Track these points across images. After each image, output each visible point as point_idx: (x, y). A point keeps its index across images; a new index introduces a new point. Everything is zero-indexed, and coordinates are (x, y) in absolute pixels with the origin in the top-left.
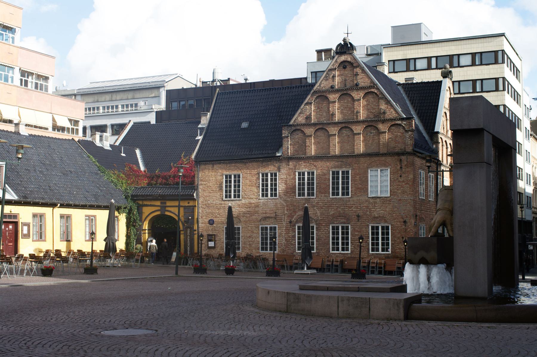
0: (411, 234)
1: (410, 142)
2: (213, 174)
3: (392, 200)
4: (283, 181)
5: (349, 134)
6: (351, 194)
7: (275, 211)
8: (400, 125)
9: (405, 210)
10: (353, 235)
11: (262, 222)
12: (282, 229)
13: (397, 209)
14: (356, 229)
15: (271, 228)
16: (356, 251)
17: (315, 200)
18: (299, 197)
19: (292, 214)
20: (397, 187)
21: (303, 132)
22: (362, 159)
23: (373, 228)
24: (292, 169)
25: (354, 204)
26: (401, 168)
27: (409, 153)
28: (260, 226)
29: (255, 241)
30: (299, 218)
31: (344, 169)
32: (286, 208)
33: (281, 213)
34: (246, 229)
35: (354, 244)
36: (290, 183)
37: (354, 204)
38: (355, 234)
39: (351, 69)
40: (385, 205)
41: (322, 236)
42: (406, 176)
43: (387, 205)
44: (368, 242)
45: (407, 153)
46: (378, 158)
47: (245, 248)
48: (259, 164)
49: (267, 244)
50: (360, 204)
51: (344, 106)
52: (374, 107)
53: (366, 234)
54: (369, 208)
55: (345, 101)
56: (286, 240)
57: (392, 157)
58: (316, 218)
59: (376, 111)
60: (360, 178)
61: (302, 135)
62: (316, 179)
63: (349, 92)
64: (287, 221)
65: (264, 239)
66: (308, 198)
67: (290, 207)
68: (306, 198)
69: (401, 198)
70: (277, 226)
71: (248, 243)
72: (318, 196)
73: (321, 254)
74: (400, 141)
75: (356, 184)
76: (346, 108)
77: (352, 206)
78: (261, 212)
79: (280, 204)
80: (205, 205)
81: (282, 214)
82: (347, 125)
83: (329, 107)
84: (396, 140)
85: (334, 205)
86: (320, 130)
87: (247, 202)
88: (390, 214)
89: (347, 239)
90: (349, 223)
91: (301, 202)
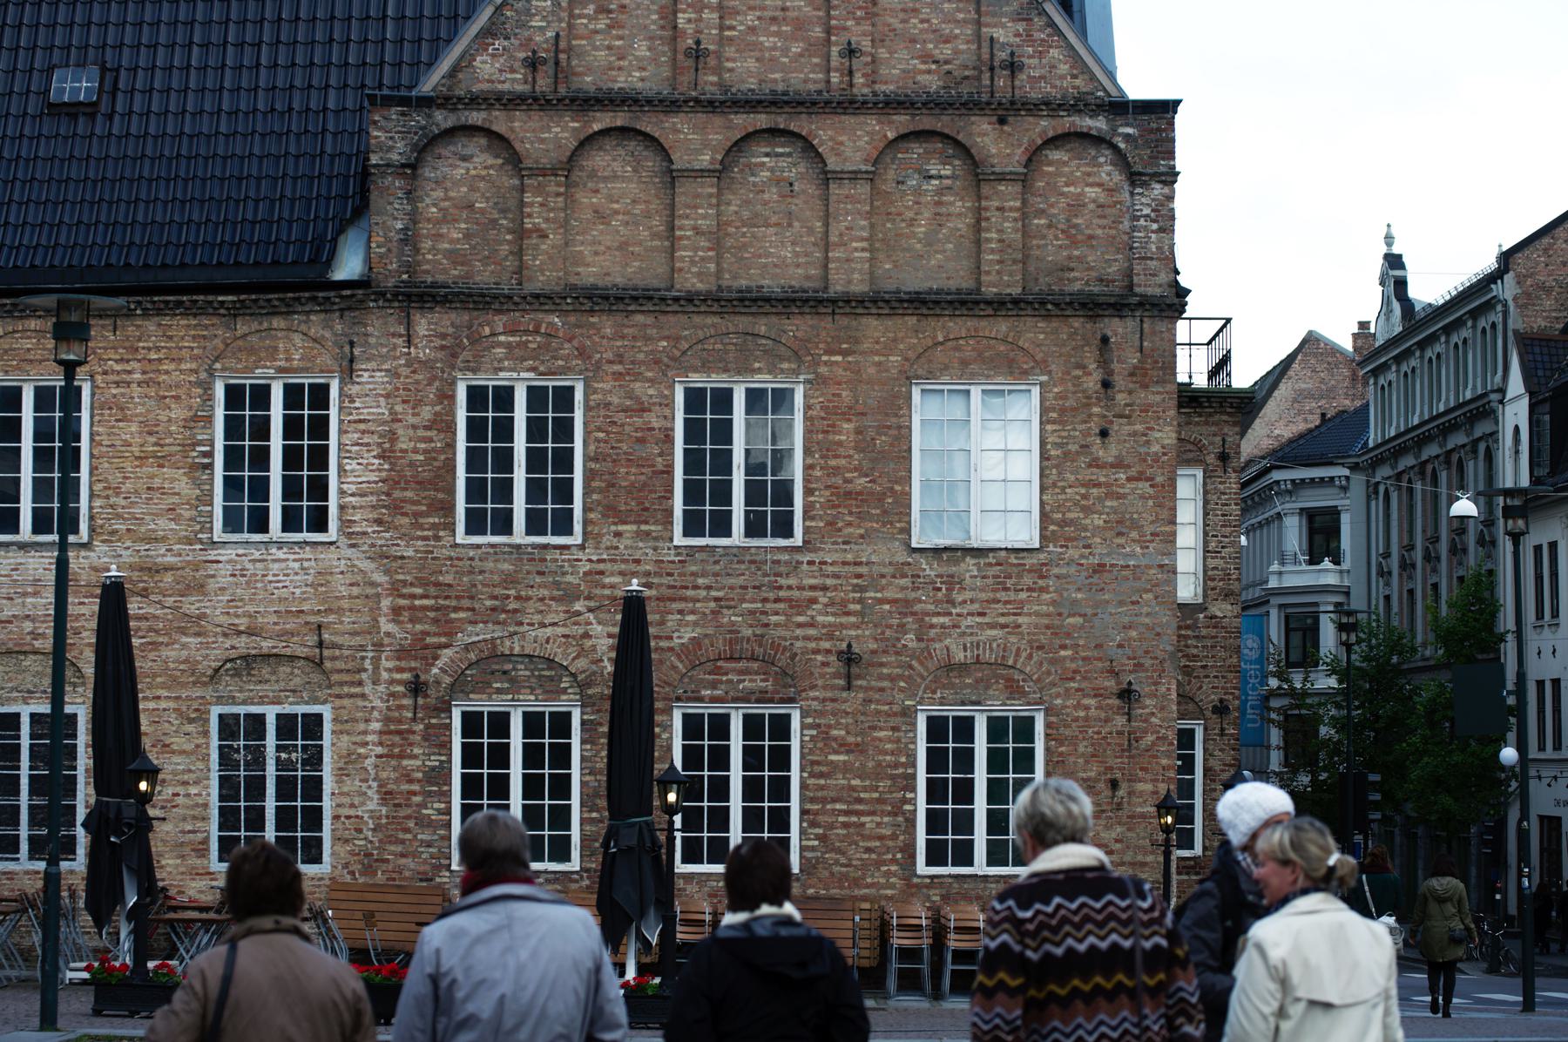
0: (1164, 762)
1: (1160, 240)
3: (1056, 571)
5: (792, 174)
6: (806, 531)
7: (312, 619)
8: (1098, 140)
10: (817, 769)
11: (228, 685)
13: (1080, 620)
14: (835, 732)
15: (286, 725)
16: (837, 862)
17: (580, 555)
19: (429, 640)
20: (1084, 497)
21: (498, 141)
22: (873, 322)
23: (936, 728)
24: (427, 364)
25: (825, 588)
26: (1106, 385)
27: (1153, 305)
28: (215, 711)
29: (180, 800)
30: (470, 666)
32: (386, 603)
33: (354, 634)
35: (821, 818)
36: (415, 451)
37: (825, 588)
40: (1012, 596)
42: (1135, 434)
43: (1023, 595)
44: (907, 807)
45: (1141, 304)
46: (970, 323)
48: (206, 327)
50: (862, 589)
52: (947, 29)
53: (896, 765)
54: (913, 614)
56: (386, 796)
57: (1055, 324)
58: (582, 663)
59: (956, 52)
60: (858, 432)
61: (490, 161)
62: (587, 433)
64: (392, 682)
66: (534, 546)
67: (413, 596)
68: (519, 547)
69: (1107, 561)
70: (327, 712)
72: (600, 535)
74: (1099, 232)
76: (774, 19)
79: (349, 578)
81: (358, 640)
83: (675, 13)
84: (1076, 226)
85: (696, 587)
86: (609, 143)
88: (1040, 648)
89: (781, 789)
90: (791, 700)
91: (490, 565)
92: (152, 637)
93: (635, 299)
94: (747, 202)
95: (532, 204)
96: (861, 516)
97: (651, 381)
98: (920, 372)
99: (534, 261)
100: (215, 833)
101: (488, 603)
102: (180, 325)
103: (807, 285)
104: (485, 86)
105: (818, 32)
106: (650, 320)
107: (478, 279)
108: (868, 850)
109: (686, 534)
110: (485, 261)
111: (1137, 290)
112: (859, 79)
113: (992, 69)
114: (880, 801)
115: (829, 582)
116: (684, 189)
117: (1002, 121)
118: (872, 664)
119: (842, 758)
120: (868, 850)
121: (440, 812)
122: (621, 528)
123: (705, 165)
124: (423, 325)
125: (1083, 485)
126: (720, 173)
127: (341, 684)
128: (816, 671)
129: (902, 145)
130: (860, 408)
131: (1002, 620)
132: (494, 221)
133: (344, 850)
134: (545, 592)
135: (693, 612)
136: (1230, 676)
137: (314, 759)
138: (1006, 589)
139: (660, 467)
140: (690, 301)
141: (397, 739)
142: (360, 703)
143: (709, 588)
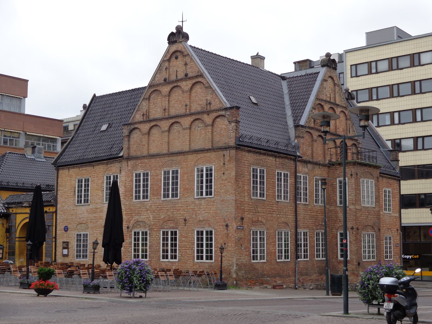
2: (69, 179)
3: (216, 201)
8: (223, 116)
13: (219, 211)
18: (136, 201)
19: (130, 219)
20: (221, 186)
23: (198, 232)
24: (130, 170)
25: (182, 207)
26: (224, 164)
31: (174, 168)
35: (181, 251)
37: (182, 207)
41: (153, 243)
42: (228, 173)
43: (211, 206)
44: (193, 248)
45: (229, 147)
46: (204, 154)
48: (104, 167)
50: (187, 207)
53: (192, 240)
57: (216, 153)
58: (149, 222)
60: (187, 177)
62: (150, 180)
63: (179, 84)
64: (125, 227)
69: (224, 199)
73: (153, 263)
75: (184, 185)
76: (177, 101)
77: (180, 209)
80: (62, 211)
85: (164, 208)
86: (155, 128)
88: (213, 217)
90: (177, 228)
91: (137, 205)
95: (143, 140)
96: (188, 193)
97: (159, 170)
98: (197, 165)
104: (137, 120)
108: (188, 257)
112: (187, 110)
113: (207, 105)
114: (189, 247)
115: (183, 205)
117: (208, 115)
118: (188, 221)
119: (184, 239)
120: (188, 257)
123: (166, 130)
124: (130, 163)
125: (220, 184)
126: (169, 131)
129: (195, 122)
130: (188, 172)
131: (208, 211)
132: (140, 144)
134: (144, 210)
135: (164, 212)
136: (354, 221)
138: (208, 205)
143: (166, 208)
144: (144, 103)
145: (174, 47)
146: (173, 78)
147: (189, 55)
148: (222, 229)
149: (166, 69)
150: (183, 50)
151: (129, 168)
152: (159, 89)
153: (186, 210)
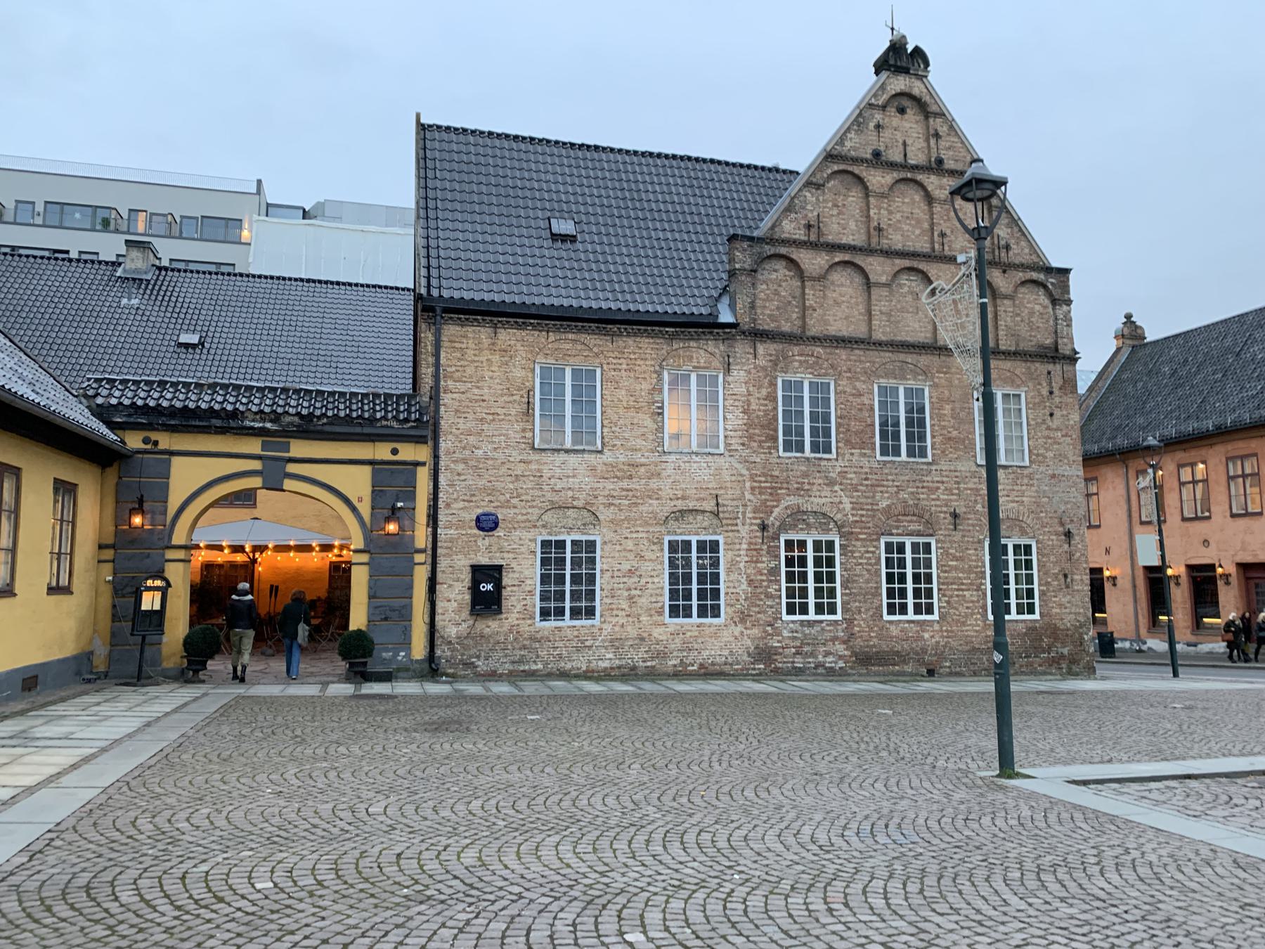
3: (1037, 477)
4: (736, 404)
6: (933, 455)
7: (714, 492)
9: (1066, 503)
10: (944, 568)
12: (738, 547)
14: (951, 551)
15: (702, 546)
17: (836, 463)
19: (768, 503)
24: (764, 369)
25: (943, 482)
26: (1051, 393)
28: (667, 539)
29: (649, 586)
32: (748, 484)
33: (734, 500)
34: (618, 547)
36: (759, 410)
37: (943, 482)
38: (949, 566)
39: (918, 118)
41: (858, 572)
42: (1063, 416)
43: (1024, 488)
47: (612, 609)
49: (688, 596)
50: (958, 483)
51: (903, 212)
53: (977, 567)
55: (906, 200)
56: (750, 582)
57: (1029, 364)
58: (839, 516)
60: (952, 410)
61: (787, 273)
62: (836, 405)
64: (752, 524)
65: (679, 580)
66: (815, 458)
67: (760, 482)
68: (808, 459)
70: (721, 539)
71: (626, 594)
72: (844, 454)
73: (859, 626)
75: (944, 427)
76: (908, 218)
78: (667, 492)
79: (731, 472)
80: (465, 461)
82: (915, 264)
86: (839, 269)
87: (622, 459)
90: (931, 535)
92: (634, 500)
93: (856, 342)
94: (899, 301)
97: (864, 382)
99: (810, 322)
100: (667, 603)
101: (796, 486)
102: (645, 342)
103: (926, 341)
104: (787, 235)
105: (926, 226)
106: (862, 353)
107: (783, 329)
108: (967, 608)
109: (881, 455)
110: (787, 320)
111: (1061, 351)
112: (946, 248)
114: (970, 584)
115: (945, 479)
116: (875, 292)
117: (1004, 272)
119: (954, 563)
120: (967, 608)
121: (776, 590)
122: (853, 451)
124: (761, 349)
127: (727, 525)
128: (941, 522)
130: (952, 399)
131: (1016, 499)
132: (790, 302)
133: (730, 610)
134: (820, 481)
135: (887, 492)
137: (715, 563)
139: (869, 422)
140: (880, 344)
141: (755, 553)
142: (737, 535)
144: (808, 194)
145: (899, 83)
146: (896, 156)
147: (944, 115)
148: (1055, 542)
149: (878, 126)
150: (927, 98)
151: (762, 362)
152: (856, 172)
153: (956, 491)
